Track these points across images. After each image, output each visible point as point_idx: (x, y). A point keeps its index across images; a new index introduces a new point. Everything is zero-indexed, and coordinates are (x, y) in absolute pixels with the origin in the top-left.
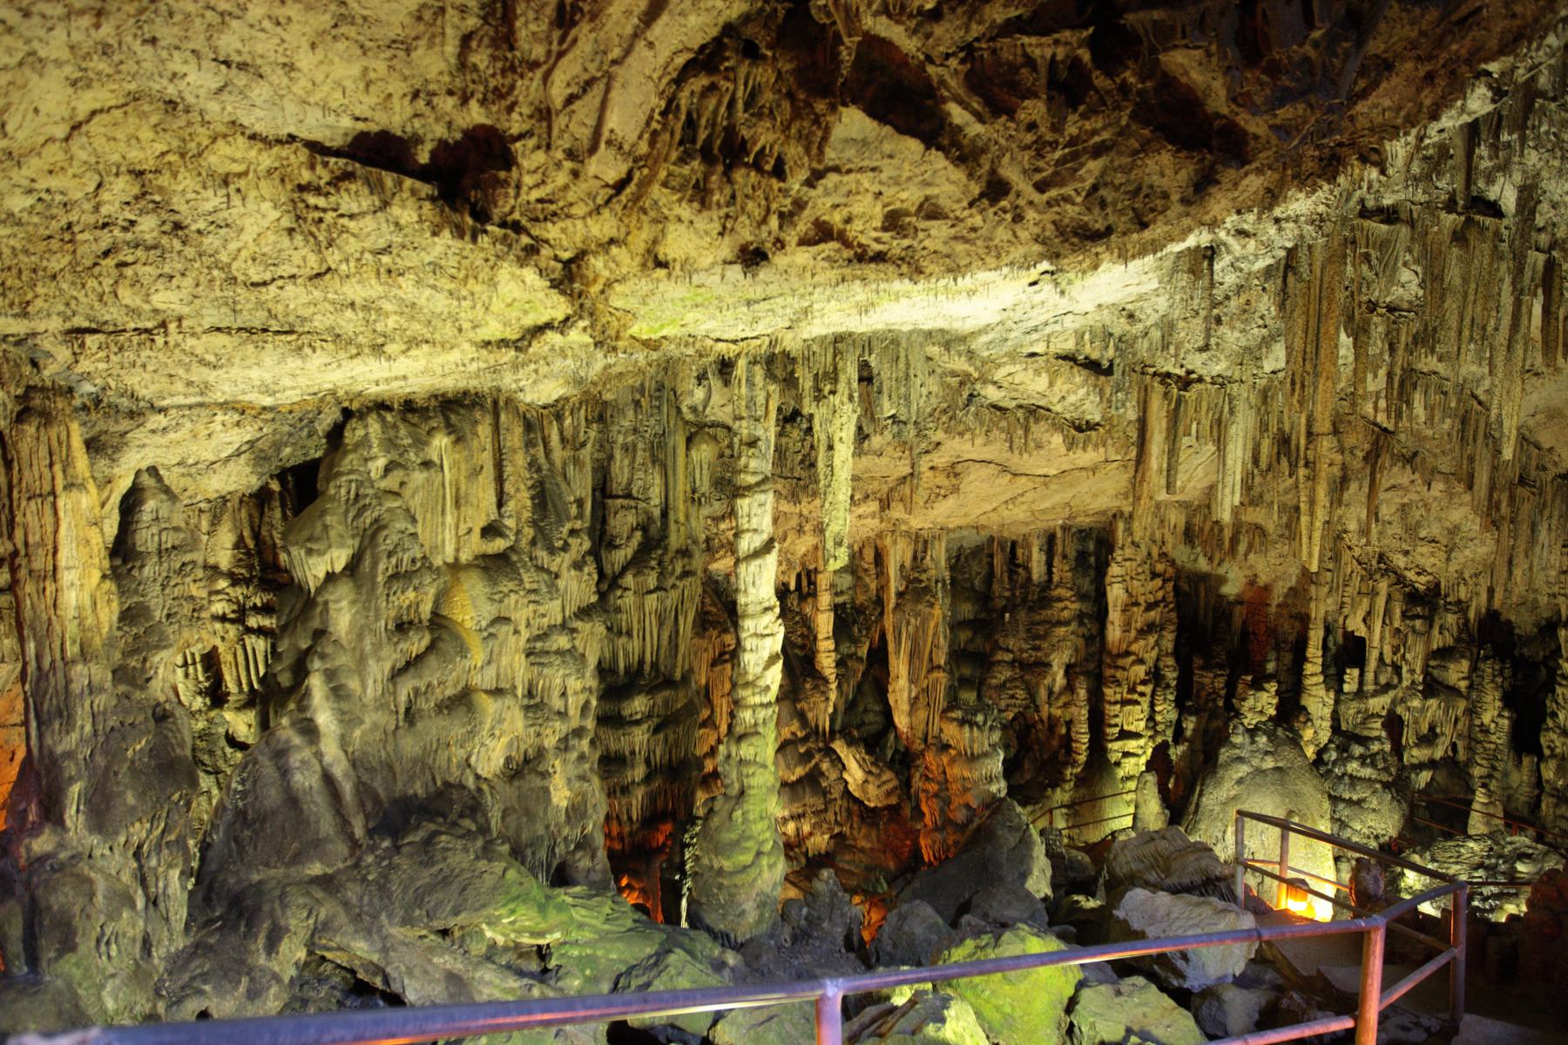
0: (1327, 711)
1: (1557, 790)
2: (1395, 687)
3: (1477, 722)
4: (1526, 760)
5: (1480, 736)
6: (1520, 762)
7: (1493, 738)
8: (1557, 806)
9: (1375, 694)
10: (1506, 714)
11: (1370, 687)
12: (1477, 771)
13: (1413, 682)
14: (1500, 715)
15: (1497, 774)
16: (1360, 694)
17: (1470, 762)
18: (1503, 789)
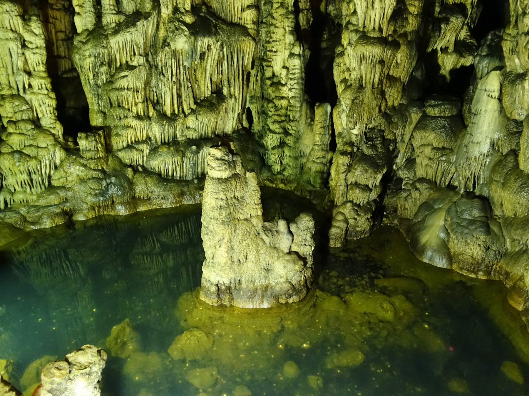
0: (37, 59)
1: (351, 144)
2: (147, 16)
3: (268, 74)
4: (319, 112)
5: (271, 92)
6: (313, 112)
7: (285, 91)
8: (350, 168)
9: (119, 28)
10: (297, 50)
11: (110, 19)
12: (271, 140)
13: (176, 10)
14: (292, 55)
15: (290, 141)
16: (98, 32)
17: (266, 129)
18: (296, 158)
